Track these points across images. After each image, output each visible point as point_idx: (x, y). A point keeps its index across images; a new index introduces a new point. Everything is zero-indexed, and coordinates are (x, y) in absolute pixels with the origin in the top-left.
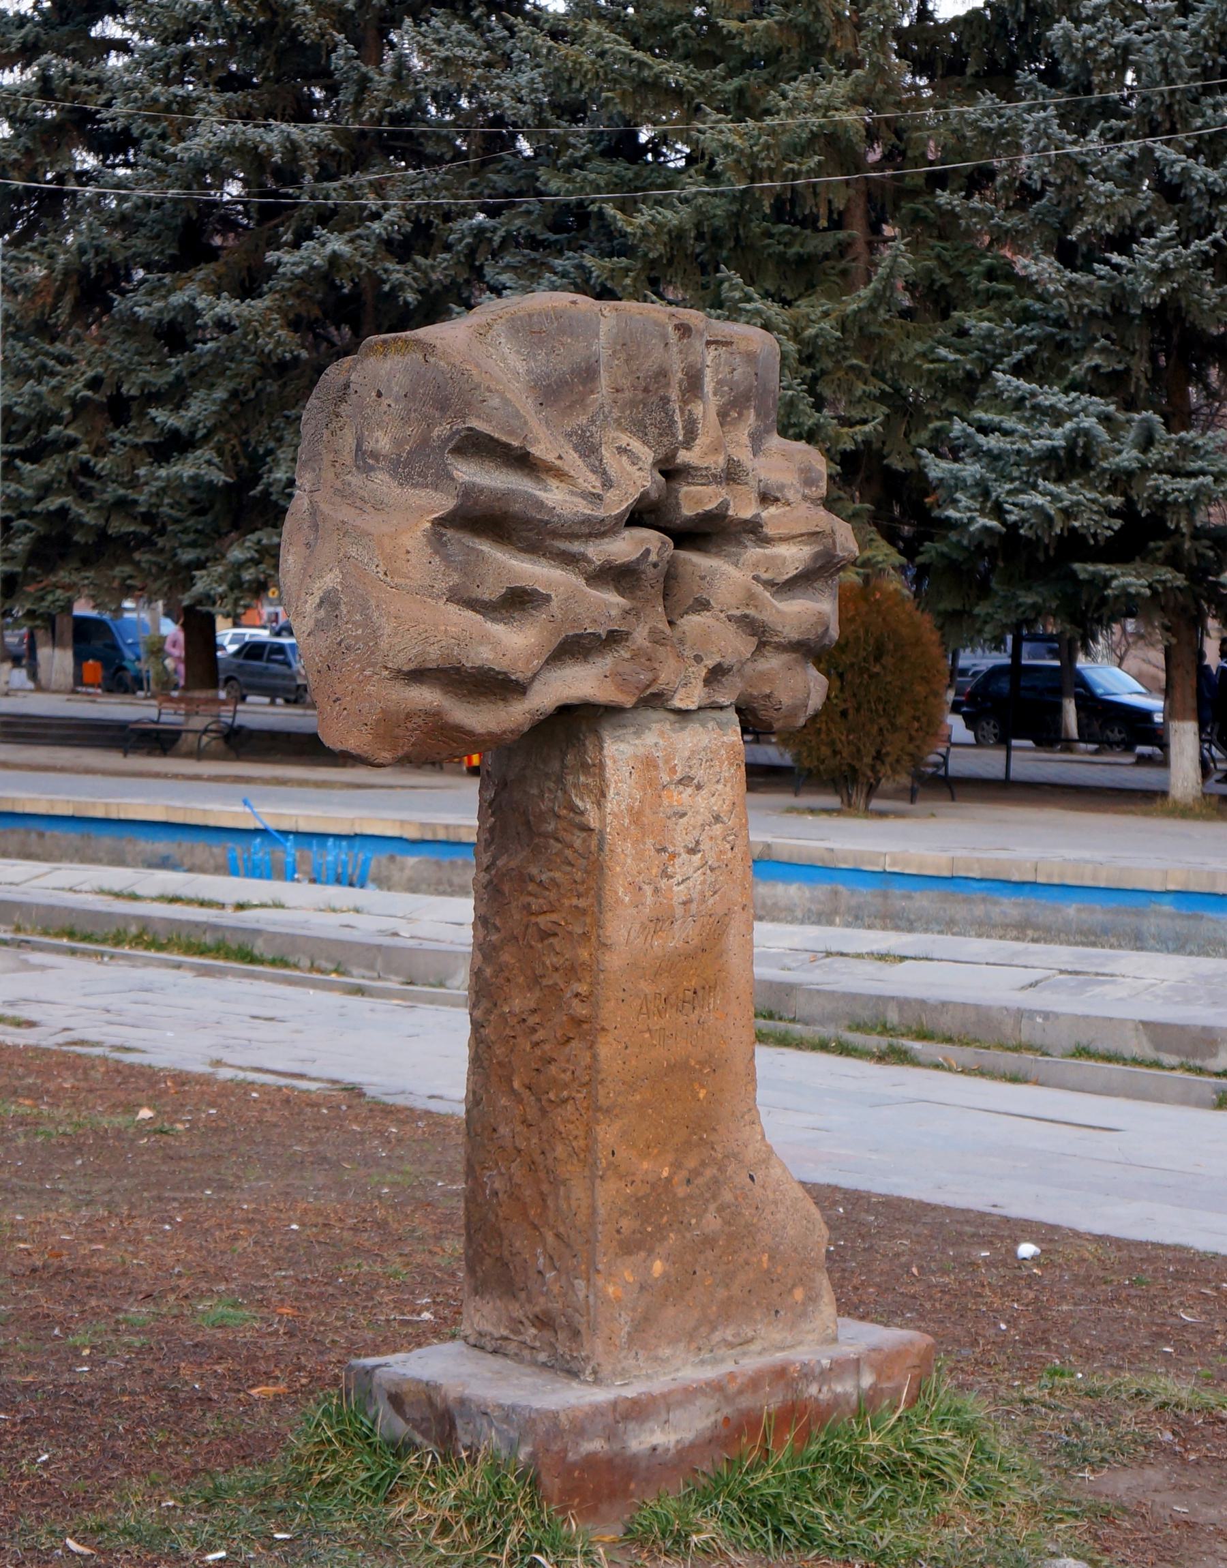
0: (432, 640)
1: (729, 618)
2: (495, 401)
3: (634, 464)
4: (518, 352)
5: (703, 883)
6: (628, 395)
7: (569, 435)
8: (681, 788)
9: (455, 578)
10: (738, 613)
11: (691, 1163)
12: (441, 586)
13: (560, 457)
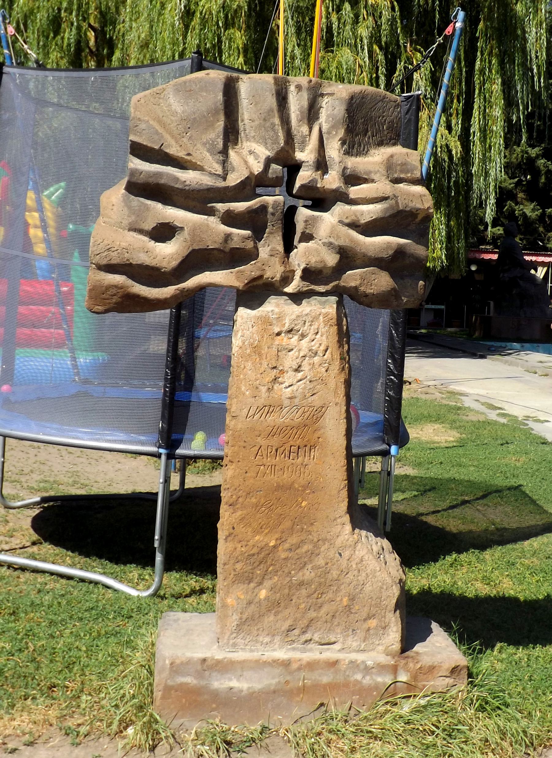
0: (113, 249)
1: (324, 244)
2: (143, 126)
3: (256, 159)
4: (179, 102)
5: (304, 388)
6: (257, 123)
7: (204, 144)
8: (290, 336)
9: (133, 218)
10: (326, 241)
11: (293, 540)
12: (125, 222)
13: (189, 154)
